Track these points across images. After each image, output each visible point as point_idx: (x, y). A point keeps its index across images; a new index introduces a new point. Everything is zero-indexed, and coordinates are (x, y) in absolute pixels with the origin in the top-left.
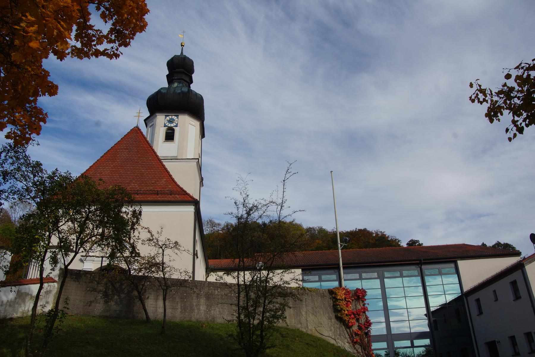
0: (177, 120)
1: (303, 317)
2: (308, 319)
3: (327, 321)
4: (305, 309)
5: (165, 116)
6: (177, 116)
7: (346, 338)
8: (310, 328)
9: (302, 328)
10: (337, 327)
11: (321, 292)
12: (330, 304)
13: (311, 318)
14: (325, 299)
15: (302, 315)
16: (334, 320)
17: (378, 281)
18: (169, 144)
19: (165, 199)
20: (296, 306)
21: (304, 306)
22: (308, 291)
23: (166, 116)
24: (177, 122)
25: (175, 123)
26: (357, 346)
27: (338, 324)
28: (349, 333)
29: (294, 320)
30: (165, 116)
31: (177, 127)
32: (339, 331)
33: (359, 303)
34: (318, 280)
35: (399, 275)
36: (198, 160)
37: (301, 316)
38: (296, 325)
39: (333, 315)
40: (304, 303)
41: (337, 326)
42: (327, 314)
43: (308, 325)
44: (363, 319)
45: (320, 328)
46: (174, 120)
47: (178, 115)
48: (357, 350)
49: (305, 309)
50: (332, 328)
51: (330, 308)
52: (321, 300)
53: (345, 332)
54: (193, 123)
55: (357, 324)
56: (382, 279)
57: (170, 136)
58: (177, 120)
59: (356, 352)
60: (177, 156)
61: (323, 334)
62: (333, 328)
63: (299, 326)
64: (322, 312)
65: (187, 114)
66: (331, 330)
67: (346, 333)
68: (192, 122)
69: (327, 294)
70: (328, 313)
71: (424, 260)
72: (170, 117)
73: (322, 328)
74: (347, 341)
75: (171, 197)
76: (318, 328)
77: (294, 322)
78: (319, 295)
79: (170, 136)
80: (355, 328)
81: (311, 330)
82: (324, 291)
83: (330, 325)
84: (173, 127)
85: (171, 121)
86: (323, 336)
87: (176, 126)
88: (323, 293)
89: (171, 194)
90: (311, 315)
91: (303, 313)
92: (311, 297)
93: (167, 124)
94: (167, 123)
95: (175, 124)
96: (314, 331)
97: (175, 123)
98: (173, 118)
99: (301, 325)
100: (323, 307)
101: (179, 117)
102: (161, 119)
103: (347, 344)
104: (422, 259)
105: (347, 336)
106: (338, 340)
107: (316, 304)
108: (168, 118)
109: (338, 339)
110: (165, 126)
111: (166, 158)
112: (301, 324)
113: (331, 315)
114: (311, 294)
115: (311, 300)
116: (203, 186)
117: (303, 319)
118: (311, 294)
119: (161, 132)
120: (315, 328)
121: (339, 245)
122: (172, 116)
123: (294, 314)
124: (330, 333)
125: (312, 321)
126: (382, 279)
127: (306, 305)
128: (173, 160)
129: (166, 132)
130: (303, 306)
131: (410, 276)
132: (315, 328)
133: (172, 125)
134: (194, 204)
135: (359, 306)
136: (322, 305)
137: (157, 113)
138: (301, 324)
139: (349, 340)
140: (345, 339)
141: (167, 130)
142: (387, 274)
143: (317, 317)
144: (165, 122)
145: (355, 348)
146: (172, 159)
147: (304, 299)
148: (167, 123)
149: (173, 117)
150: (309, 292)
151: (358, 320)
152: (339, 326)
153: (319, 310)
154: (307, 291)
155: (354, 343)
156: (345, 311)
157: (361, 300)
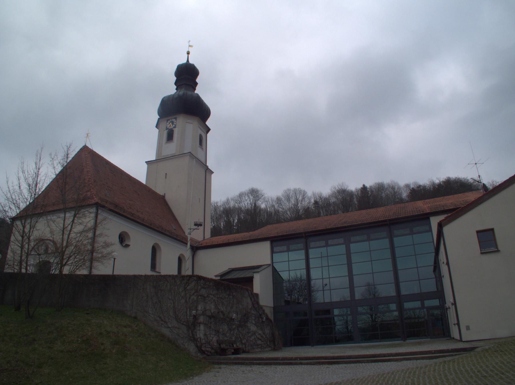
0: (175, 122)
6: (176, 118)
23: (168, 121)
24: (175, 124)
25: (174, 125)
34: (325, 245)
56: (347, 244)
58: (175, 122)
60: (175, 154)
84: (173, 129)
87: (175, 127)
93: (168, 127)
97: (174, 125)
98: (173, 120)
101: (177, 119)
110: (167, 129)
122: (172, 119)
126: (347, 244)
128: (171, 158)
149: (173, 119)
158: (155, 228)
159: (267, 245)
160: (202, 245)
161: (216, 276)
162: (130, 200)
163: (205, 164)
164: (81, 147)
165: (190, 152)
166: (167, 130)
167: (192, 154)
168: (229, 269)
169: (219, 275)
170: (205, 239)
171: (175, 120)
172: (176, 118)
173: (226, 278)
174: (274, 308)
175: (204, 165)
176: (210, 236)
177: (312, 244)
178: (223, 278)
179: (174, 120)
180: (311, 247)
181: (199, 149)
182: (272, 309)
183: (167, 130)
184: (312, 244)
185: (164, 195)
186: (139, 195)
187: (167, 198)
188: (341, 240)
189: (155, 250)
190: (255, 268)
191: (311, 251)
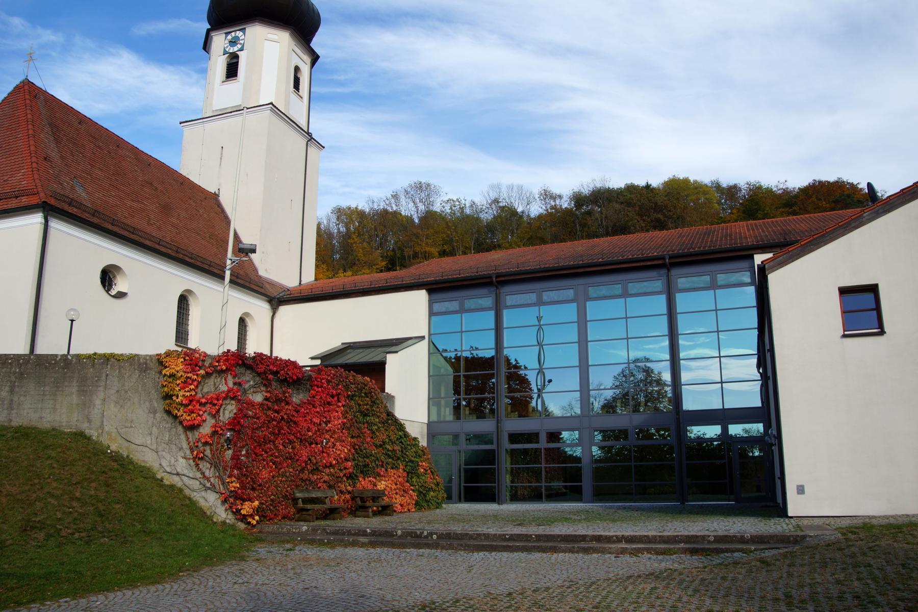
1: (96, 409)
2: (105, 413)
3: (145, 415)
4: (101, 395)
5: (226, 33)
6: (243, 30)
7: (181, 449)
8: (106, 429)
9: (91, 429)
10: (165, 427)
11: (141, 360)
12: (158, 383)
13: (112, 410)
14: (149, 374)
15: (94, 406)
16: (160, 415)
17: (573, 306)
18: (233, 85)
19: (5, 206)
20: (85, 389)
21: (101, 389)
22: (114, 360)
24: (242, 42)
25: (240, 44)
26: (204, 466)
27: (168, 423)
28: (191, 439)
29: (76, 415)
30: (226, 33)
31: (243, 50)
32: (167, 436)
33: (225, 380)
35: (619, 292)
36: (271, 106)
37: (92, 407)
38: (79, 424)
39: (160, 405)
40: (102, 384)
41: (167, 426)
42: (147, 404)
43: (105, 424)
44: (227, 412)
45: (127, 429)
46: (237, 38)
47: (245, 29)
48: (203, 474)
49: (103, 394)
50: (155, 430)
51: (156, 391)
52: (139, 376)
53: (183, 437)
54: (275, 37)
55: (213, 421)
57: (232, 71)
58: (243, 37)
59: (200, 476)
60: (240, 105)
61: (133, 442)
62: (156, 430)
63: (84, 427)
64: (136, 400)
65: (259, 22)
66: (151, 434)
67: (184, 439)
68: (270, 36)
69: (153, 365)
70: (151, 401)
71: (670, 258)
72: (233, 34)
73: (133, 429)
74: (183, 455)
75: (16, 201)
76: (124, 430)
77: (76, 419)
78: (136, 367)
79: (232, 71)
80: (206, 429)
81: (109, 433)
82: (148, 358)
83: (150, 423)
85: (233, 42)
86: (133, 445)
87: (241, 50)
88: (146, 364)
89: (17, 197)
90: (112, 405)
91: (98, 402)
92: (117, 371)
93: (227, 50)
94: (227, 47)
95: (239, 46)
96: (114, 435)
97: (240, 44)
99: (90, 425)
100: (140, 389)
101: (247, 30)
102: (220, 41)
103: (181, 460)
104: (667, 257)
105: (185, 445)
106: (164, 453)
107: (126, 384)
108: (229, 37)
109: (164, 451)
111: (225, 112)
112: (89, 421)
113: (156, 405)
114: (120, 366)
115: (118, 377)
116: (324, 148)
117: (95, 413)
118: (120, 366)
119: (219, 64)
120: (116, 428)
121: (229, 262)
123: (77, 405)
124: (149, 438)
125: (113, 417)
127: (105, 388)
129: (228, 65)
130: (99, 389)
131: (732, 285)
132: (116, 428)
133: (236, 49)
134: (42, 209)
135: (224, 385)
136: (140, 386)
137: (211, 33)
138: (89, 421)
139: (188, 452)
140: (180, 450)
141: (231, 59)
142: (592, 292)
143: (124, 408)
144: (226, 46)
145: (199, 469)
146: (231, 112)
147: (104, 375)
148: (227, 47)
149: (238, 32)
150: (116, 361)
151: (214, 416)
152: (170, 425)
153: (131, 395)
154: (112, 359)
155: (198, 459)
156: (177, 398)
157: (231, 374)
158: (187, 259)
159: (420, 297)
160: (292, 296)
161: (312, 358)
162: (133, 201)
163: (306, 131)
164: (18, 82)
165: (271, 104)
166: (227, 55)
167: (275, 107)
168: (343, 344)
169: (320, 356)
170: (302, 283)
171: (241, 33)
172: (243, 30)
173: (333, 363)
174: (430, 424)
175: (304, 131)
176: (313, 278)
177: (510, 300)
178: (327, 363)
179: (239, 34)
180: (508, 304)
181: (293, 97)
182: (425, 427)
183: (227, 55)
184: (510, 300)
185: (217, 193)
186: (156, 189)
187: (223, 199)
188: (570, 293)
189: (183, 301)
190: (394, 344)
191: (506, 314)
